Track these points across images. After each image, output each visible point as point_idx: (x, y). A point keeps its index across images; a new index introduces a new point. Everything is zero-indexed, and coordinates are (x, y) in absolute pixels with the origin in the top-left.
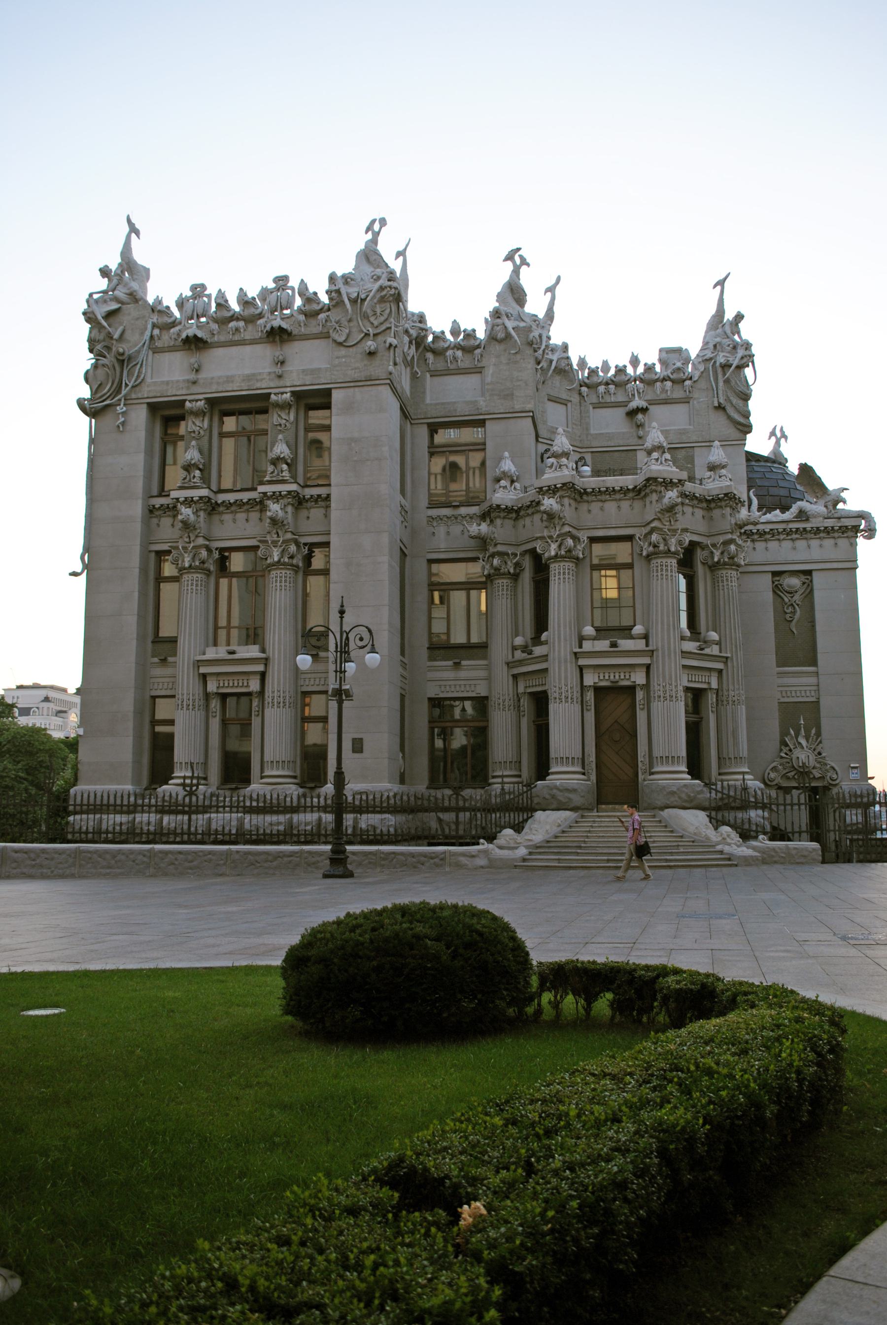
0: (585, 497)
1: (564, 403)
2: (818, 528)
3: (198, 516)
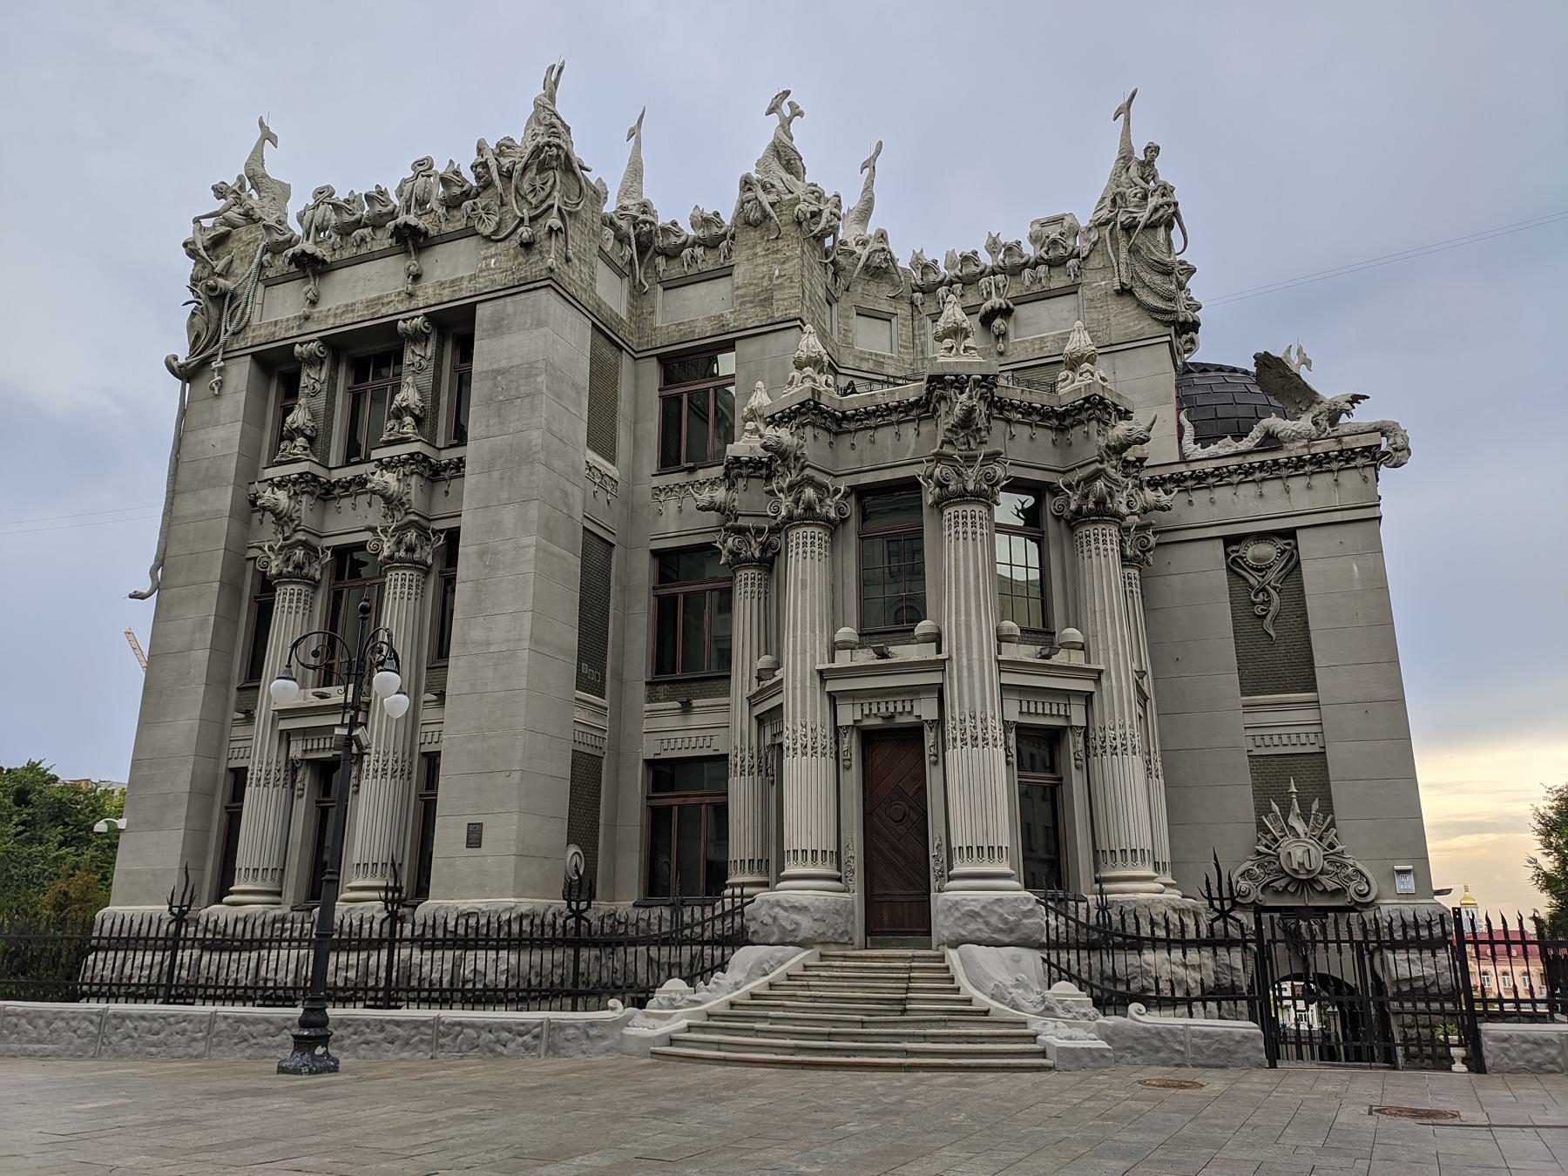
1: (887, 318)
2: (1299, 458)
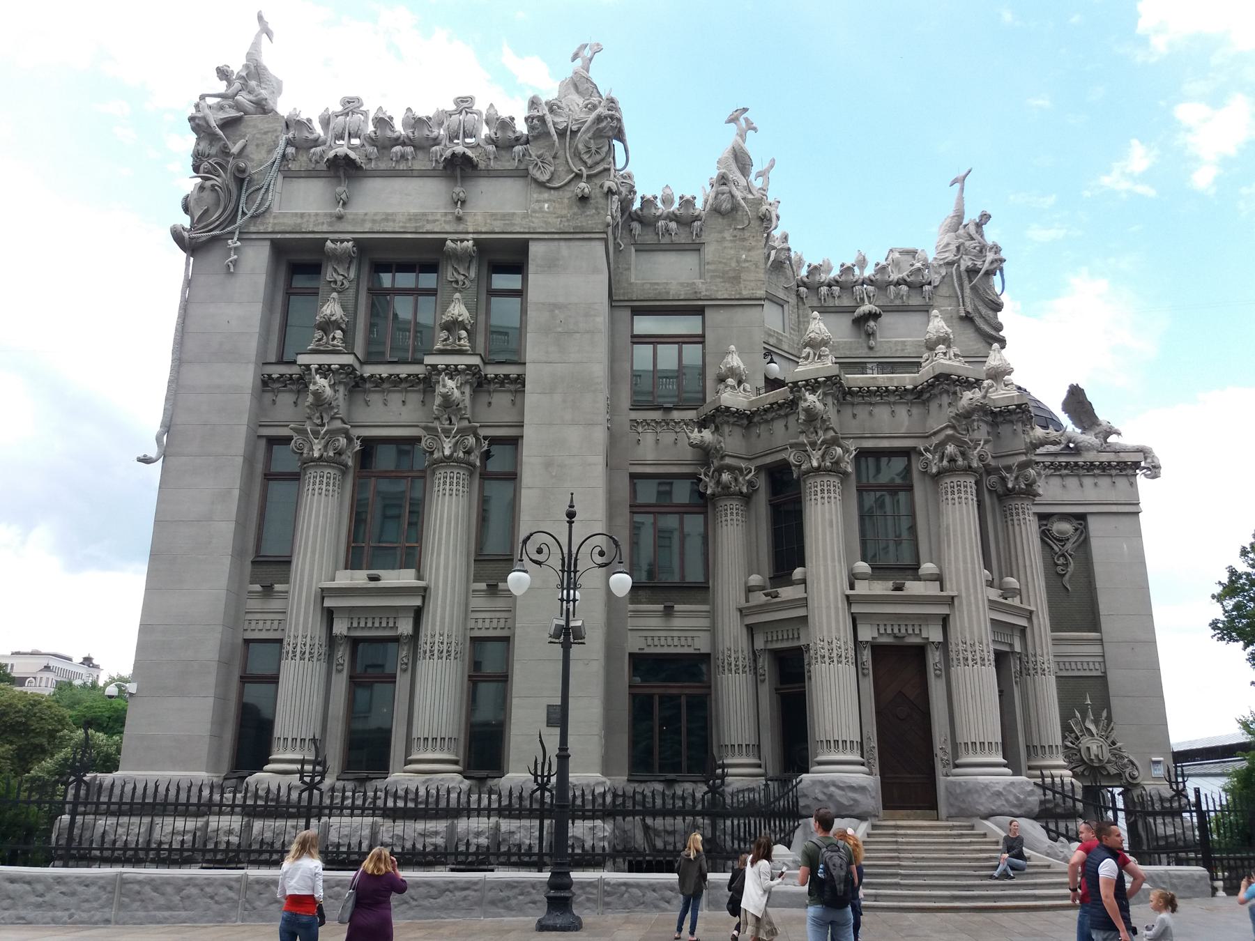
0: (848, 398)
1: (781, 304)
3: (336, 391)
